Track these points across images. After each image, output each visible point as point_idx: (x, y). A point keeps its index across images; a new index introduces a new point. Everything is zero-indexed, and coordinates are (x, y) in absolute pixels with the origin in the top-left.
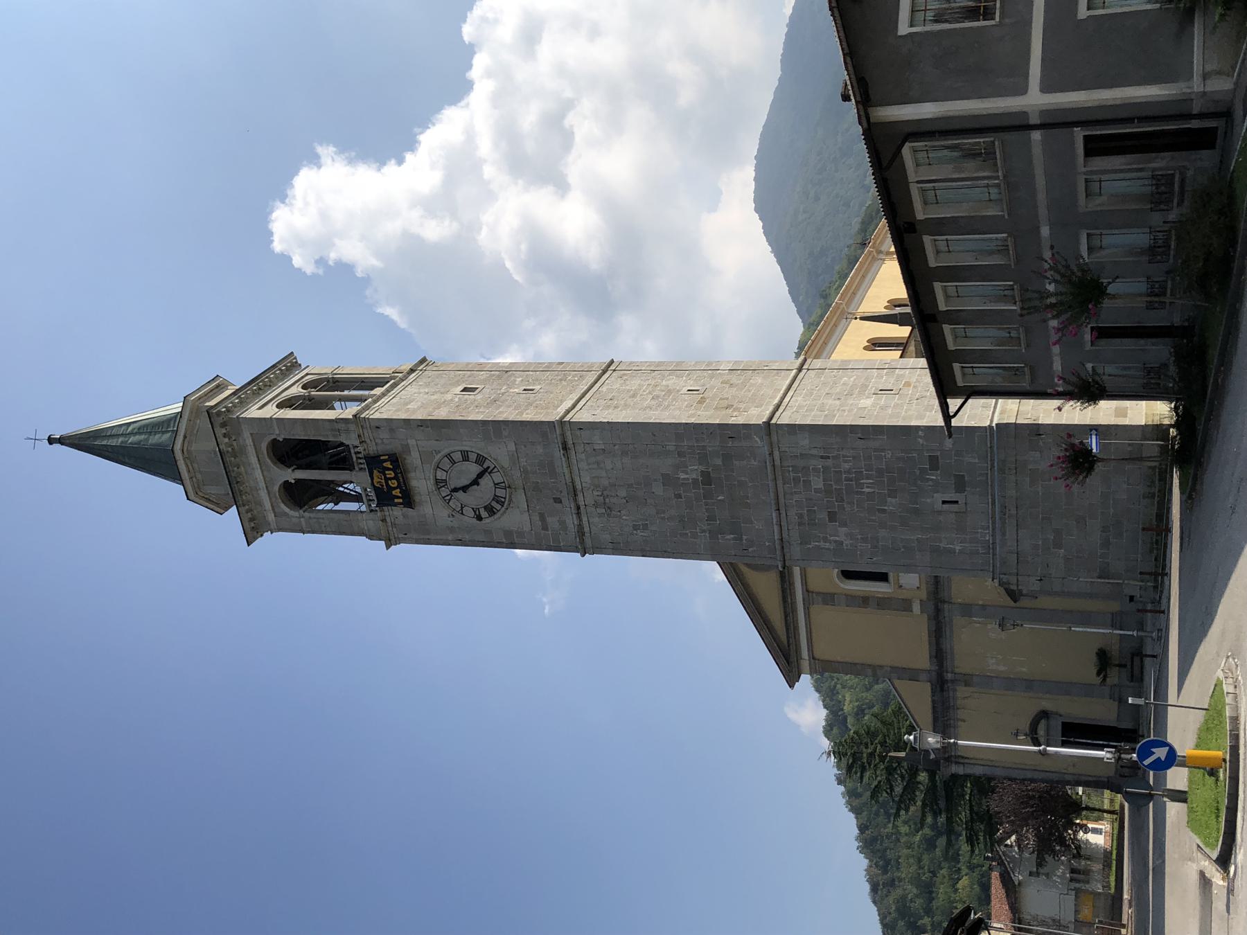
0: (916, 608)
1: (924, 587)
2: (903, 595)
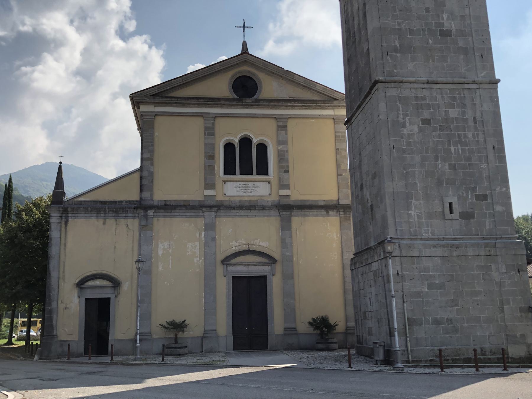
0: (209, 192)
1: (227, 199)
2: (218, 183)
